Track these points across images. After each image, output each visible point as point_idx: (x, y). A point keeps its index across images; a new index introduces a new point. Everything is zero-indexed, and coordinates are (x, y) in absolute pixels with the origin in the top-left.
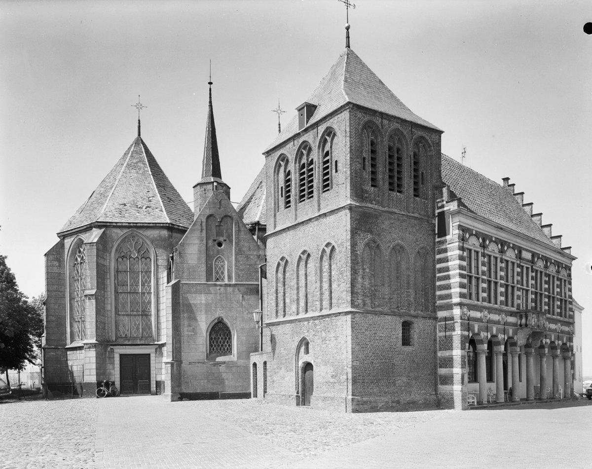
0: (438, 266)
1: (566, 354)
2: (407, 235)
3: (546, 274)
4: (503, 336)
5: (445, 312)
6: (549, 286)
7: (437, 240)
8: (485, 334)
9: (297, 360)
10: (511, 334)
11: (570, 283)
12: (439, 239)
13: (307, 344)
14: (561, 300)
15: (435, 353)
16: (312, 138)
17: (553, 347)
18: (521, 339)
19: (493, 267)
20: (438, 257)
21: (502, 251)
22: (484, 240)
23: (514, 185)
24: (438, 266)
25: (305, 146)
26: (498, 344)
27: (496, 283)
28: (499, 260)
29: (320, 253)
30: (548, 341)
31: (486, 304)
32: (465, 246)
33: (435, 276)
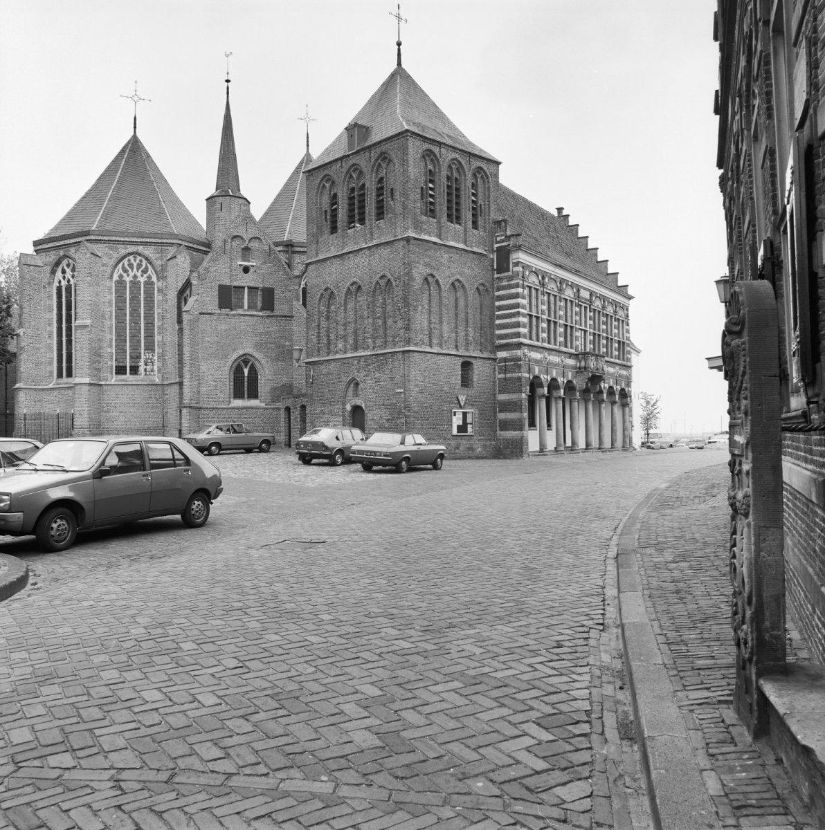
0: (497, 303)
1: (624, 400)
2: (466, 270)
3: (603, 314)
4: (546, 377)
5: (505, 352)
6: (607, 327)
7: (496, 276)
9: (344, 404)
10: (570, 378)
11: (628, 325)
12: (499, 275)
13: (357, 384)
14: (619, 342)
16: (363, 162)
17: (611, 392)
18: (580, 383)
19: (552, 306)
20: (497, 294)
21: (560, 290)
22: (543, 278)
23: (568, 215)
24: (497, 303)
25: (355, 167)
27: (624, 343)
28: (558, 298)
29: (373, 286)
30: (607, 386)
31: (546, 345)
32: (526, 284)
33: (494, 314)
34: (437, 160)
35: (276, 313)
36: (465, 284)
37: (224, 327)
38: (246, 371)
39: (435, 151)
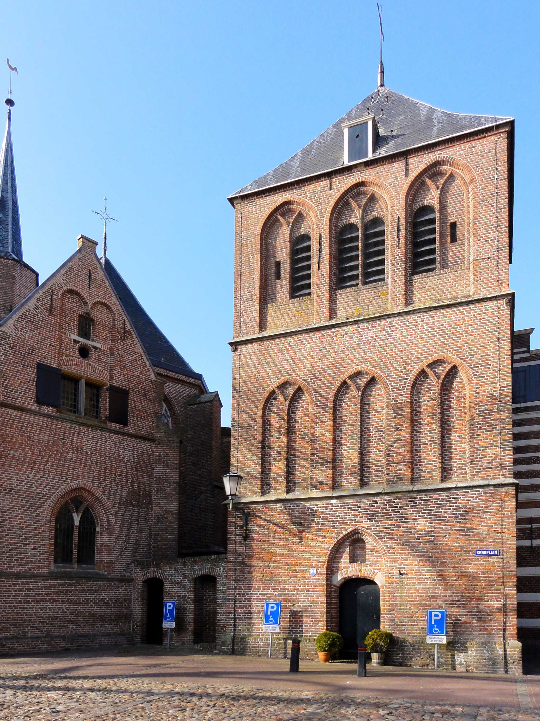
35: (130, 429)
37: (44, 438)
38: (77, 519)
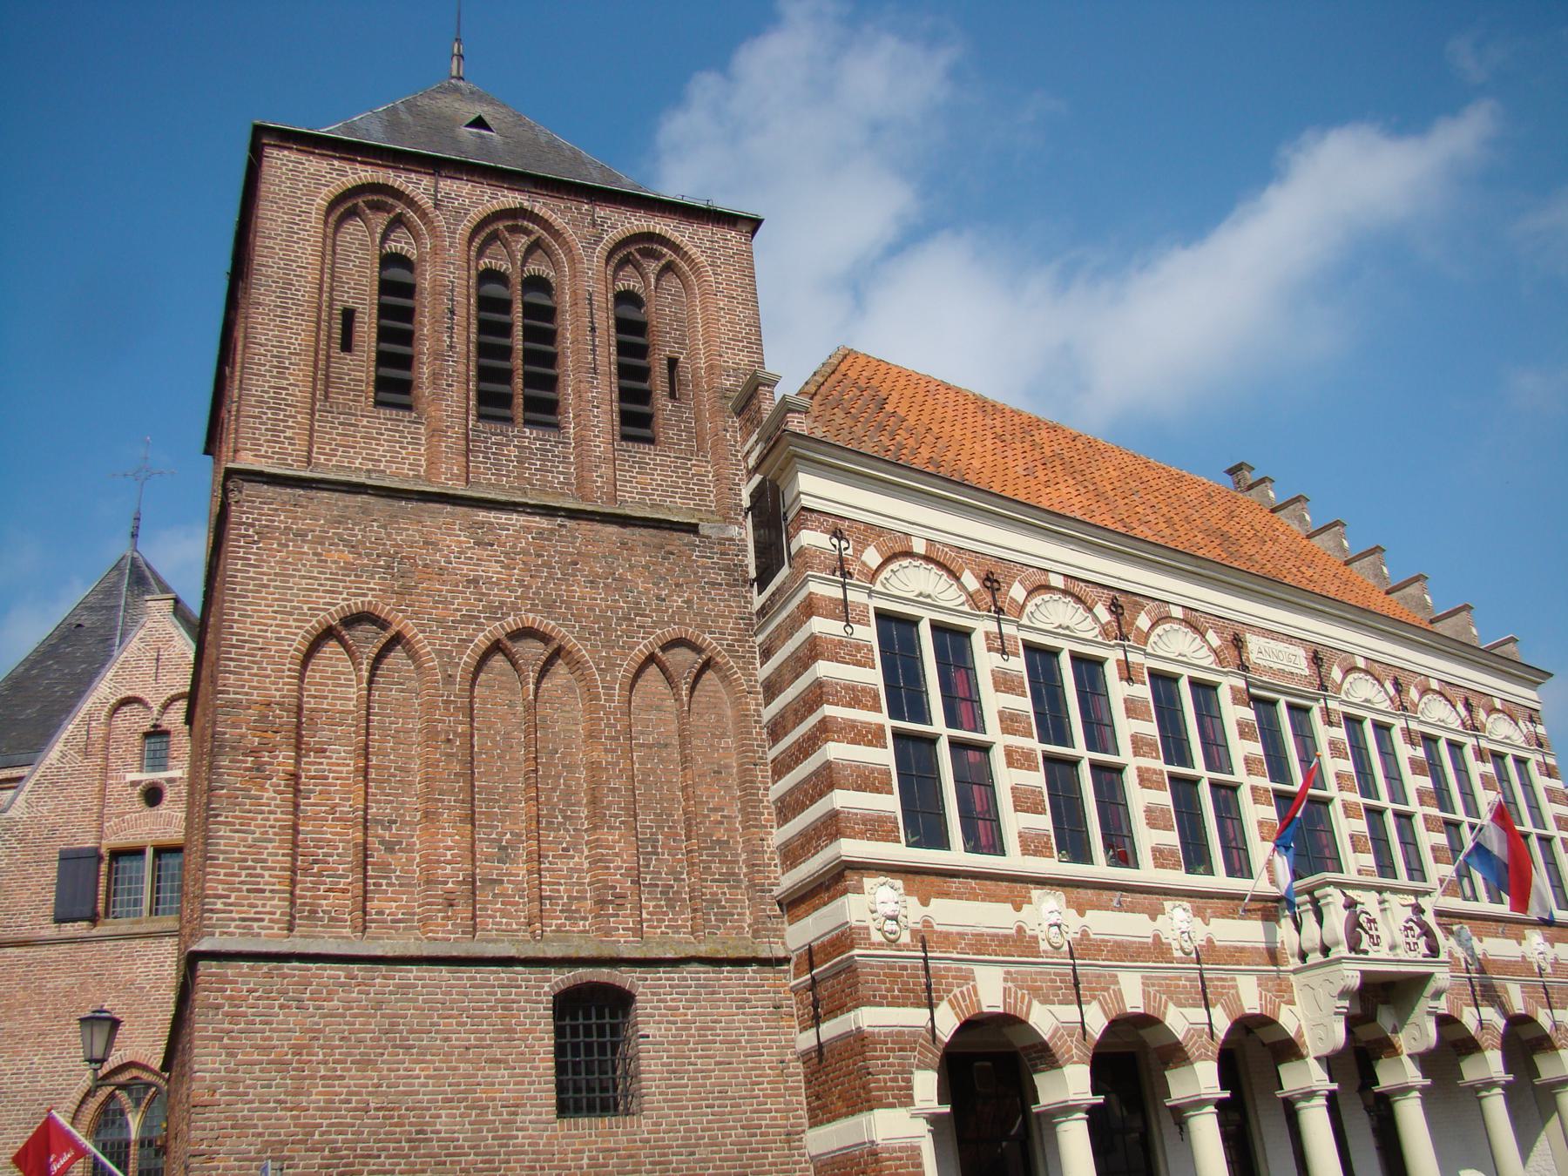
8: (1070, 1013)
15: (792, 1136)
21: (1120, 631)
26: (1175, 1054)
34: (423, 215)
36: (572, 642)
37: (63, 982)
39: (409, 189)
